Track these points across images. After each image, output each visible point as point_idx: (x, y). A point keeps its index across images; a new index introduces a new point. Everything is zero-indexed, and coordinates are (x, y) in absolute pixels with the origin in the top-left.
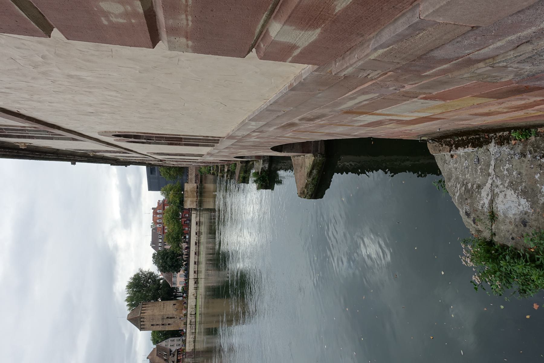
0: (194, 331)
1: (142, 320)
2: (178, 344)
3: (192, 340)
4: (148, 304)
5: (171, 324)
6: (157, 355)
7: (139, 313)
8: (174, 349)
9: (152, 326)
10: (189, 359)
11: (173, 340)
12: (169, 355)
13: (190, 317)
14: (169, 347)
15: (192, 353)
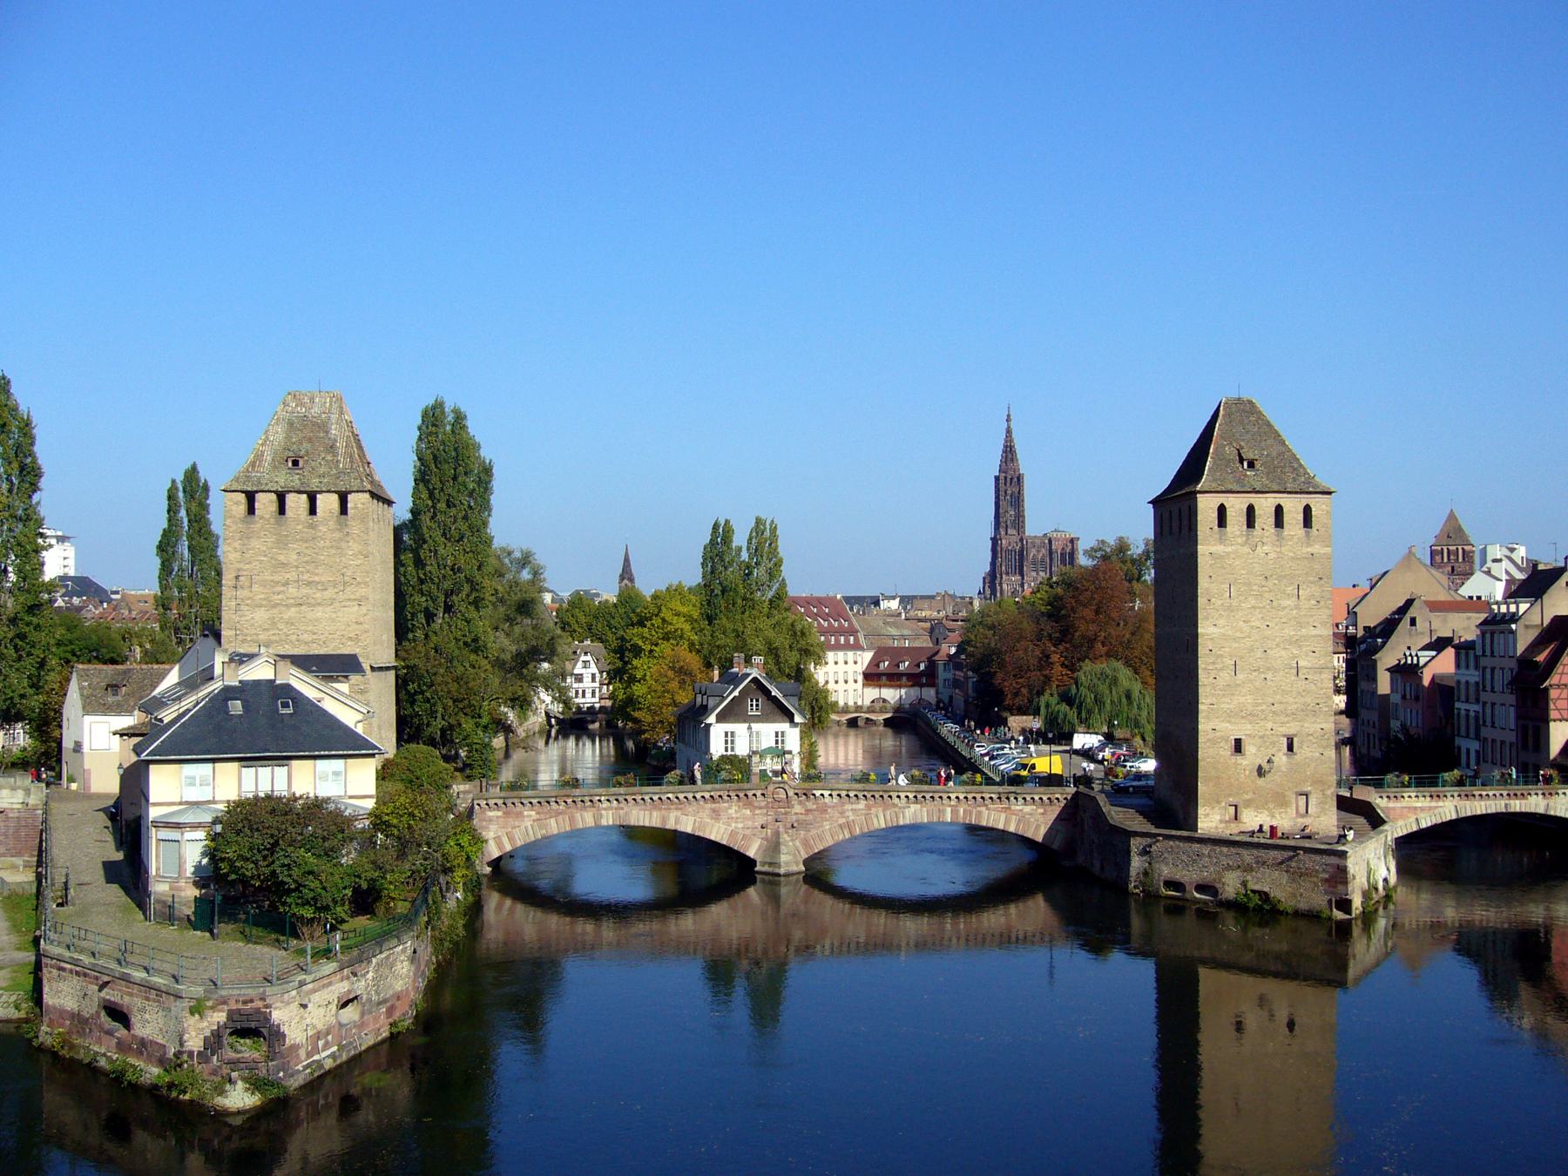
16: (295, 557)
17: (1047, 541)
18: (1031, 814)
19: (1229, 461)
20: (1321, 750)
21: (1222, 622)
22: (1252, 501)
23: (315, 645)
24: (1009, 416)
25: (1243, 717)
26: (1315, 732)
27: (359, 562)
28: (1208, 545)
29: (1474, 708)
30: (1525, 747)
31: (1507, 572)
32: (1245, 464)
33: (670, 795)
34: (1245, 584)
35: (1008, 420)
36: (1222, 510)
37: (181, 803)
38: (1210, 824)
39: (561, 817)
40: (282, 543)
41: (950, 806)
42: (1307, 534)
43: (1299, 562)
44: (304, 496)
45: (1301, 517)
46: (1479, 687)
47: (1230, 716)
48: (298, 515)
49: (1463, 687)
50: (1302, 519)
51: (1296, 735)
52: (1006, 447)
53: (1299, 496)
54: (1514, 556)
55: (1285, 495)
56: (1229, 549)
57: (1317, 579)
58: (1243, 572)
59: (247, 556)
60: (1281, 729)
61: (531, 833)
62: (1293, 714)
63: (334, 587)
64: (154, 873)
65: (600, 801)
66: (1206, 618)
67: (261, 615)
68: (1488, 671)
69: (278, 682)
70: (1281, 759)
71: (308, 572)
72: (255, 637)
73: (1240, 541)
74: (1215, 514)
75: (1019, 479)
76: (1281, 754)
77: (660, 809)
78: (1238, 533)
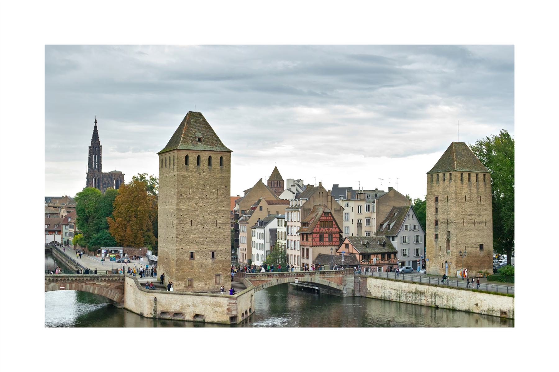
0: (403, 299)
1: (448, 175)
2: (407, 253)
3: (387, 295)
4: (485, 187)
5: (436, 242)
6: (394, 208)
7: (464, 167)
8: (396, 244)
9: (434, 198)
10: (352, 284)
11: (418, 242)
12: (386, 235)
13: (430, 291)
14: (402, 233)
15: (364, 291)
17: (111, 175)
18: (103, 286)
19: (190, 137)
20: (225, 257)
21: (186, 204)
22: (200, 154)
24: (96, 120)
25: (194, 244)
26: (223, 249)
28: (181, 171)
29: (286, 242)
30: (303, 257)
31: (297, 190)
32: (197, 139)
34: (196, 188)
35: (96, 122)
36: (187, 157)
38: (180, 288)
41: (69, 283)
42: (221, 169)
43: (217, 180)
45: (219, 161)
46: (287, 234)
47: (189, 243)
49: (280, 234)
50: (219, 162)
51: (215, 251)
52: (94, 133)
53: (218, 153)
54: (299, 184)
55: (213, 152)
56: (190, 174)
57: (224, 187)
58: (195, 183)
60: (210, 248)
62: (214, 242)
66: (180, 202)
68: (290, 227)
70: (210, 261)
73: (194, 170)
74: (185, 159)
75: (100, 148)
76: (209, 258)
78: (193, 167)
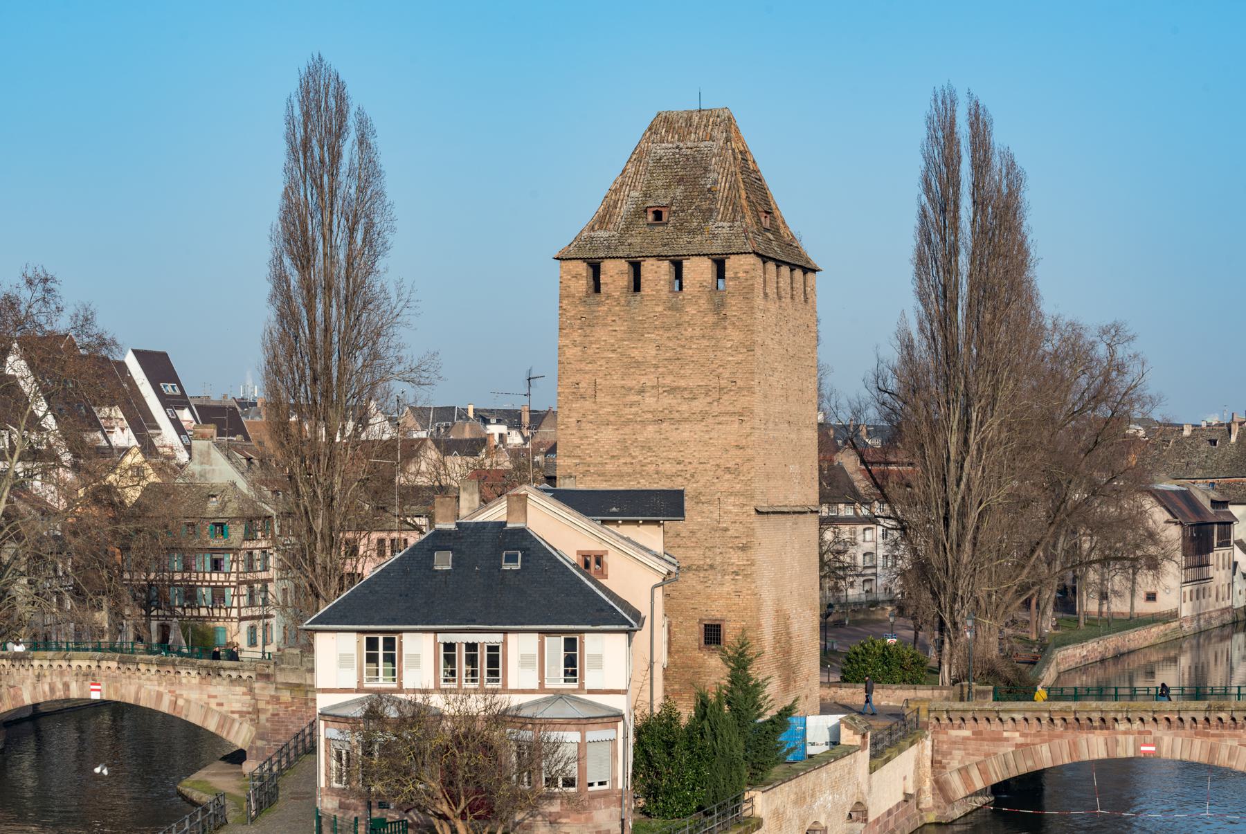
16: (654, 352)
23: (680, 480)
27: (740, 357)
33: (1223, 715)
37: (358, 691)
39: (1057, 741)
40: (636, 333)
44: (666, 264)
48: (658, 291)
59: (590, 352)
61: (1012, 764)
63: (707, 394)
64: (323, 784)
65: (1116, 720)
67: (608, 436)
69: (509, 525)
71: (671, 373)
72: (600, 468)
77: (1207, 735)
